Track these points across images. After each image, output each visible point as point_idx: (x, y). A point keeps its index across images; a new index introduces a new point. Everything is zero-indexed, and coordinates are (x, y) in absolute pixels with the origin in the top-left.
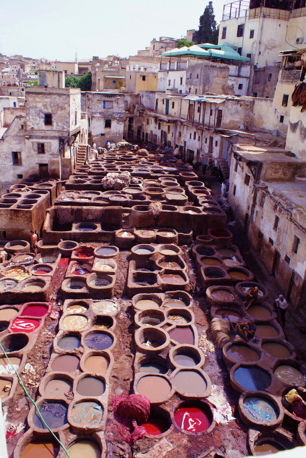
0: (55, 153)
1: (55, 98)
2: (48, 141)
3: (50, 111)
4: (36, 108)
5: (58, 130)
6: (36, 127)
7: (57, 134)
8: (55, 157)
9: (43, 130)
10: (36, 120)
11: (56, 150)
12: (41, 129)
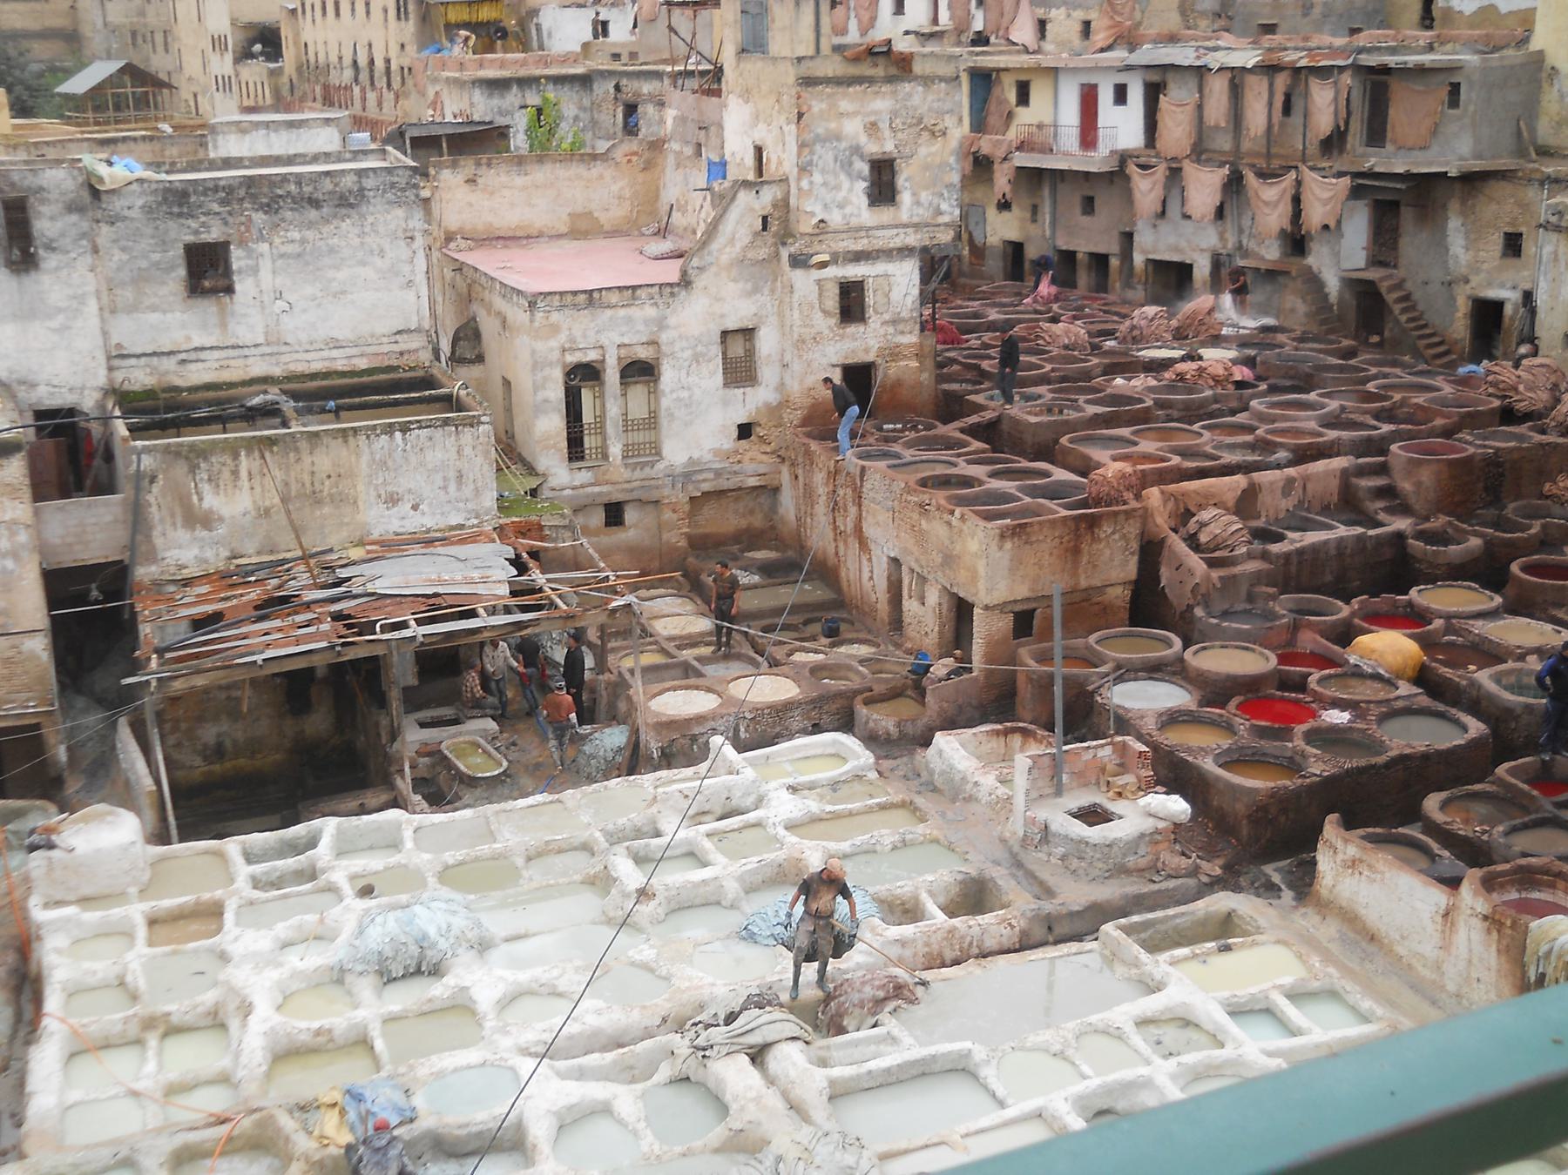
0: (904, 314)
1: (910, 95)
2: (880, 267)
3: (889, 147)
4: (838, 138)
5: (916, 220)
6: (835, 219)
7: (912, 239)
8: (902, 333)
9: (860, 229)
10: (838, 187)
11: (909, 300)
12: (854, 222)
